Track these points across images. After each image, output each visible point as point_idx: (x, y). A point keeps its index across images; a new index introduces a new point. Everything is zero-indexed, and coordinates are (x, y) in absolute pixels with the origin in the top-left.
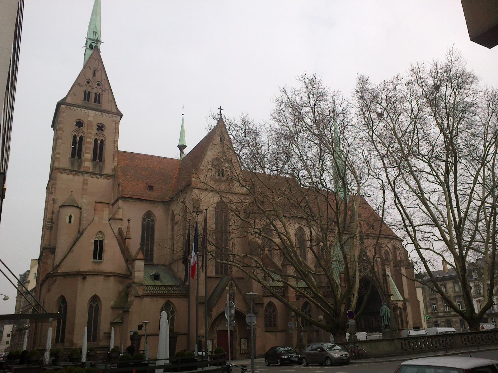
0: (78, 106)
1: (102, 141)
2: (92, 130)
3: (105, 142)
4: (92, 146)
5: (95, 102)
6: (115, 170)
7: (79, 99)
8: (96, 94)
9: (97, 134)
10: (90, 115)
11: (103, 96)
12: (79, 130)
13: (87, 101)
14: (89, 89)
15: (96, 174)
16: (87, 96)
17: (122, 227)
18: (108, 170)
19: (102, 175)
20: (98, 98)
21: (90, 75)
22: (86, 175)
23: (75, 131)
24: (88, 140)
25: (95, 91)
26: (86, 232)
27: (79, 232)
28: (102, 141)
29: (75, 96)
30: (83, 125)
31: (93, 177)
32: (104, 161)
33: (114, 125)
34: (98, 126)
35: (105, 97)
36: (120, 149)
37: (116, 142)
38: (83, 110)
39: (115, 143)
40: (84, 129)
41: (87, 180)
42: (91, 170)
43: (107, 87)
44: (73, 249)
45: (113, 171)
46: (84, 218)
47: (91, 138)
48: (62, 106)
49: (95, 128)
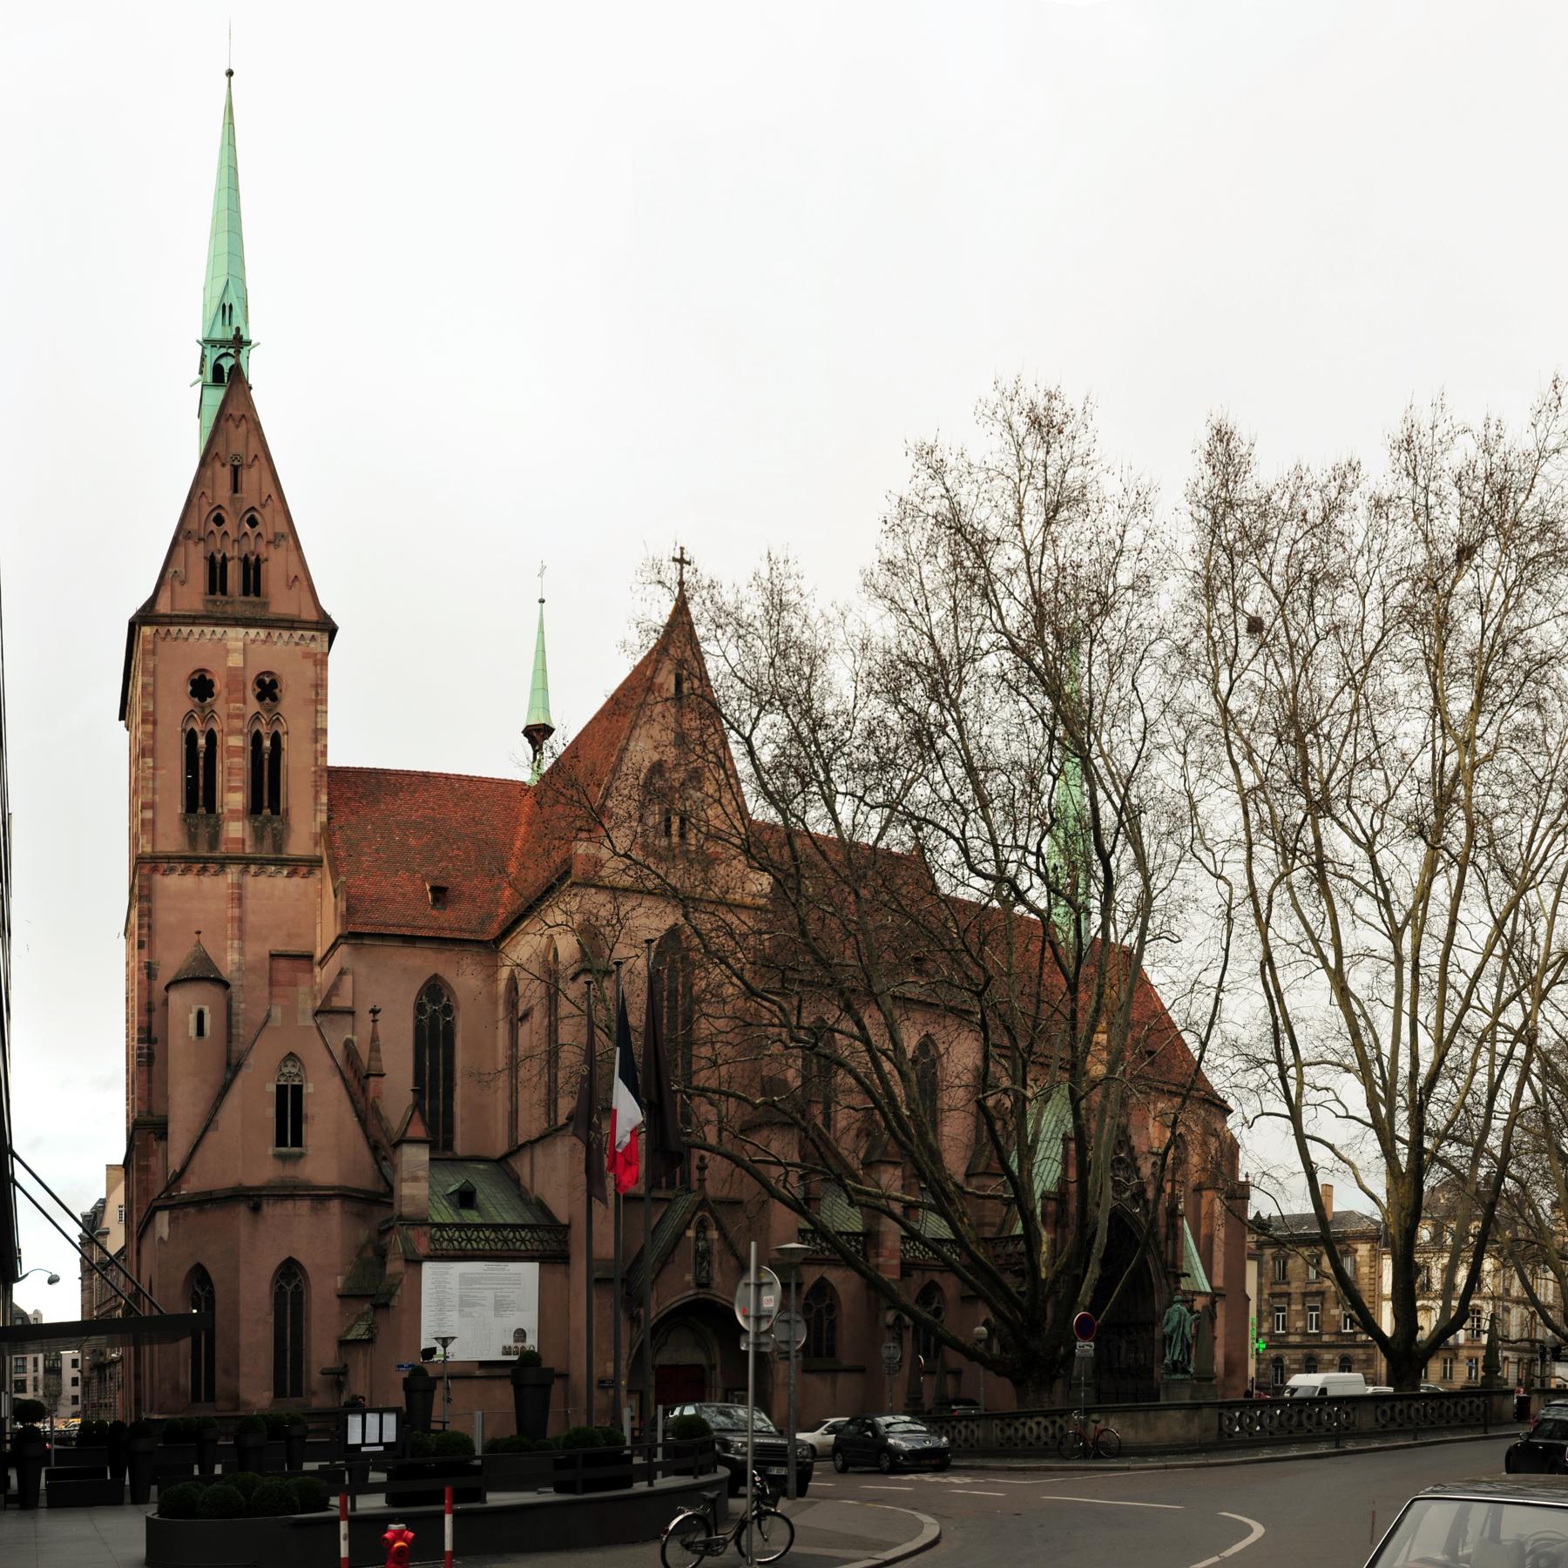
0: (193, 620)
3: (284, 740)
7: (193, 597)
10: (231, 645)
12: (203, 709)
13: (218, 593)
19: (281, 862)
26: (252, 1060)
27: (228, 1064)
28: (276, 739)
31: (256, 875)
36: (335, 759)
37: (320, 733)
38: (208, 630)
39: (316, 741)
45: (316, 844)
46: (240, 1018)
48: (147, 631)
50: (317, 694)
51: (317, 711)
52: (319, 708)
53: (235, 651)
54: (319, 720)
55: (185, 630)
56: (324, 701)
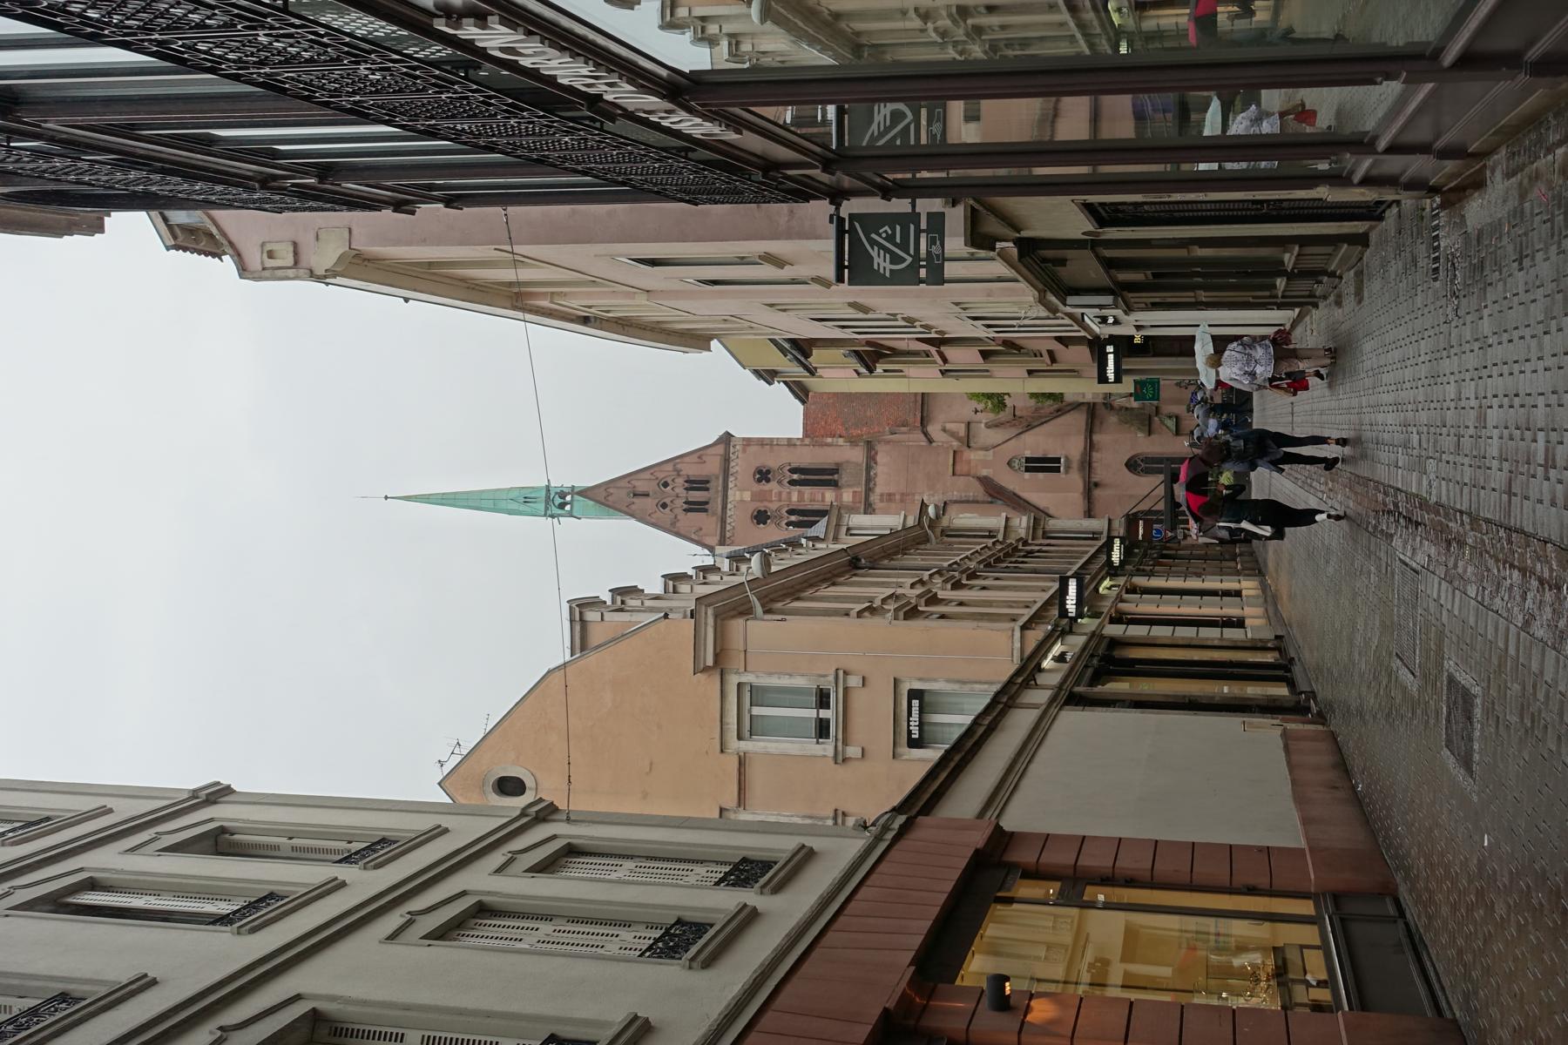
0: (723, 522)
1: (793, 471)
2: (771, 491)
3: (793, 465)
4: (807, 490)
5: (707, 489)
6: (853, 442)
7: (708, 522)
8: (686, 489)
9: (780, 482)
10: (738, 498)
14: (680, 502)
15: (869, 480)
17: (984, 421)
18: (857, 455)
21: (649, 504)
22: (872, 498)
24: (795, 498)
25: (680, 491)
28: (793, 471)
29: (701, 529)
30: (763, 509)
32: (837, 464)
33: (753, 449)
34: (759, 481)
35: (693, 471)
37: (790, 443)
38: (729, 513)
39: (795, 445)
41: (882, 495)
42: (861, 489)
43: (669, 467)
44: (1041, 508)
45: (857, 445)
47: (789, 493)
49: (766, 486)
55: (728, 527)
56: (772, 440)
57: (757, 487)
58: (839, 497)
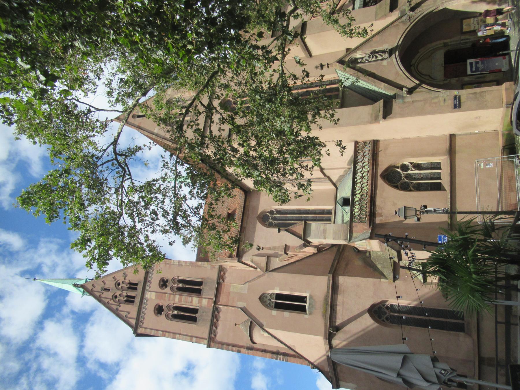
3: (180, 278)
7: (132, 310)
9: (172, 288)
11: (130, 279)
16: (130, 300)
20: (133, 286)
23: (167, 316)
30: (161, 304)
39: (182, 265)
40: (164, 303)
50: (168, 264)
51: (173, 264)
52: (172, 263)
53: (151, 295)
54: (175, 263)
57: (160, 290)
58: (200, 302)
